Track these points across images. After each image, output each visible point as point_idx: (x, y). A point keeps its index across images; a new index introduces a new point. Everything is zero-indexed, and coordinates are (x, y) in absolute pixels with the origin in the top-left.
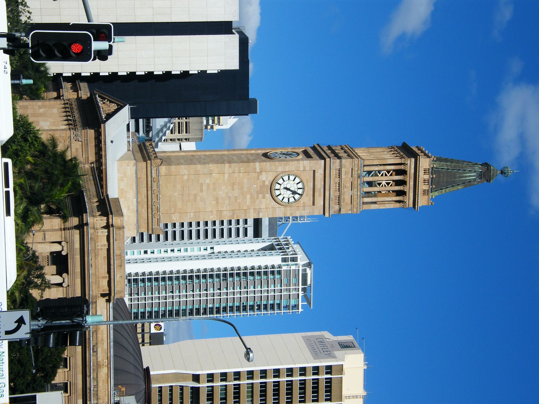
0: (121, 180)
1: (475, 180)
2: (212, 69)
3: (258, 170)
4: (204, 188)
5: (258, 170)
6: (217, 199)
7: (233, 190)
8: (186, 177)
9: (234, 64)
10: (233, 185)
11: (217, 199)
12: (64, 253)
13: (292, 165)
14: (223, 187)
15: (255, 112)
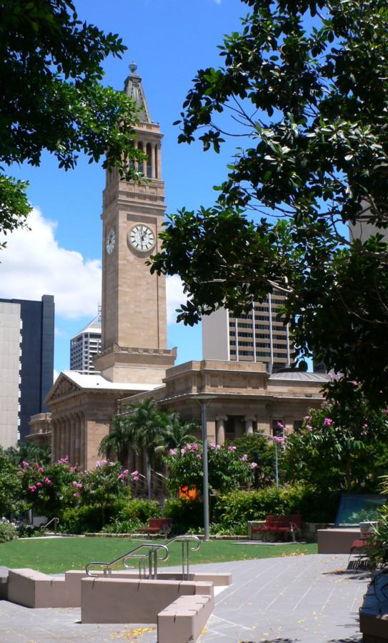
0: (130, 381)
1: (139, 90)
2: (20, 325)
3: (125, 262)
4: (138, 310)
5: (125, 262)
6: (148, 300)
7: (140, 285)
8: (129, 325)
9: (18, 307)
10: (137, 285)
11: (148, 300)
12: (226, 419)
13: (122, 233)
14: (138, 293)
15: (52, 297)
